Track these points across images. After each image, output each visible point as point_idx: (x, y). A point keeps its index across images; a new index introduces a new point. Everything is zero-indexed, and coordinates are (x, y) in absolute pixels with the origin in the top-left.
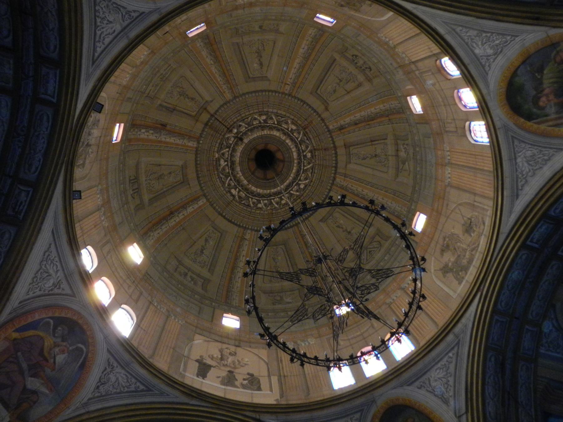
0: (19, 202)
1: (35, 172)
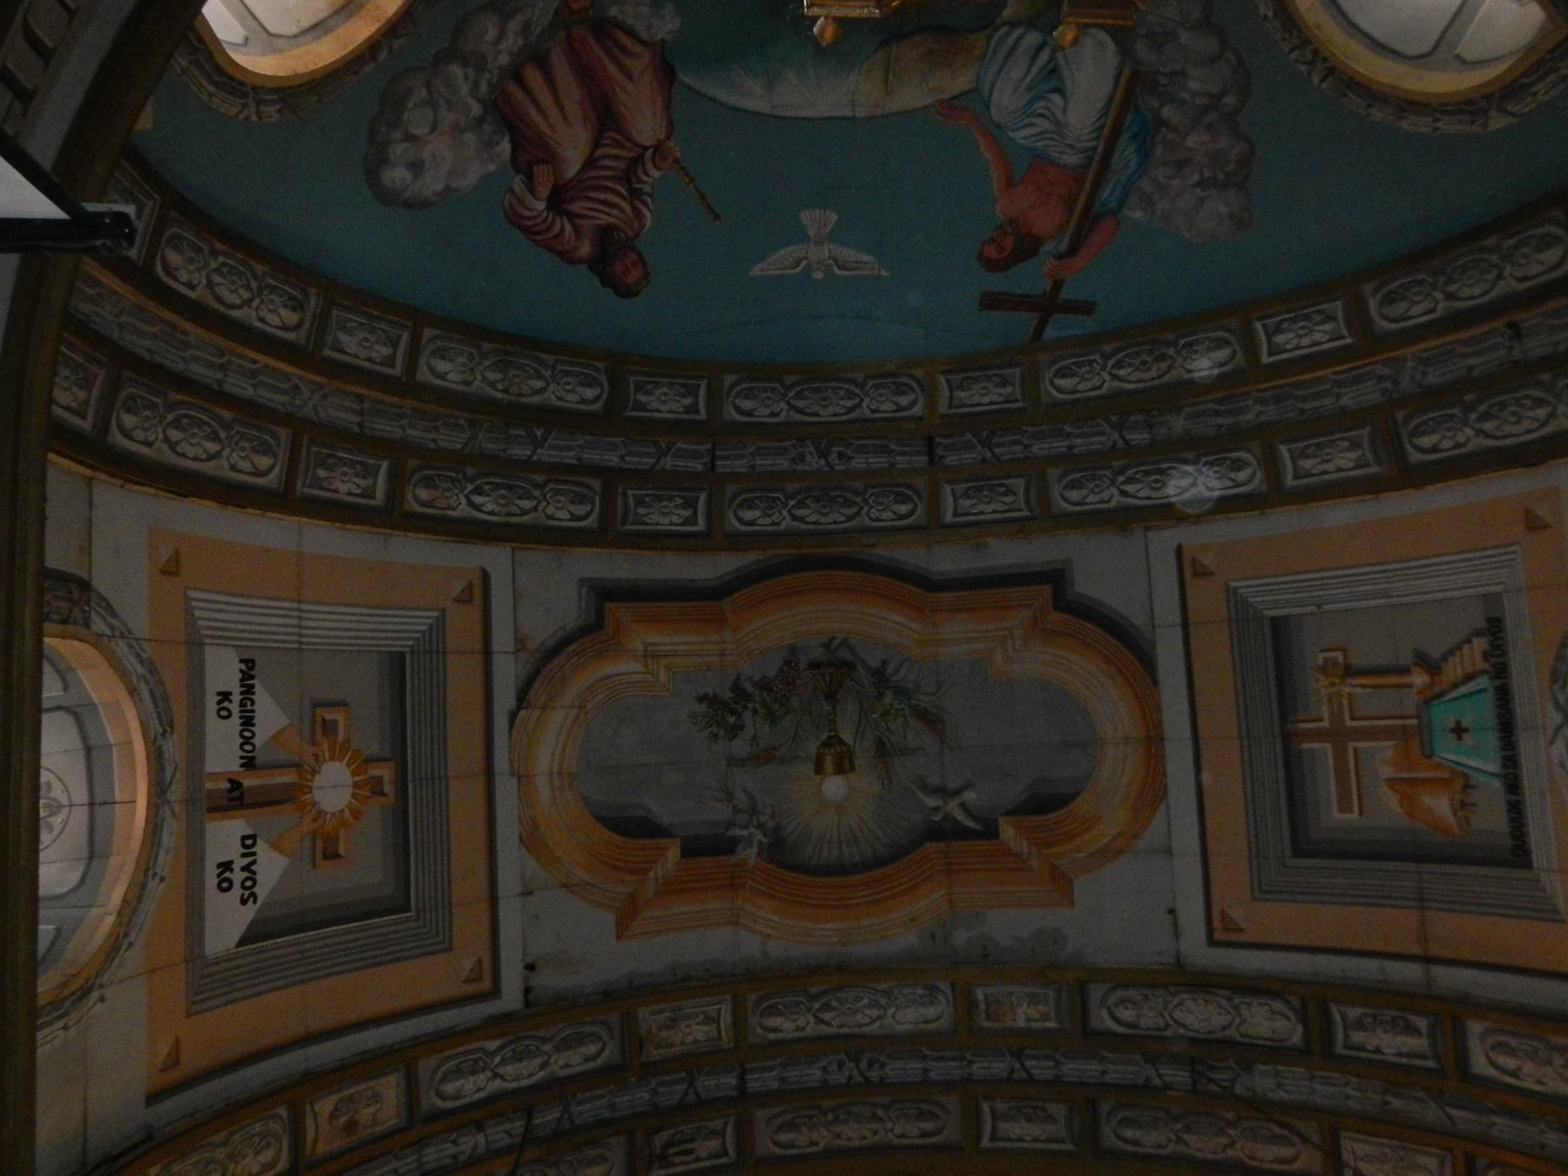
0: (690, 1146)
1: (777, 1144)
